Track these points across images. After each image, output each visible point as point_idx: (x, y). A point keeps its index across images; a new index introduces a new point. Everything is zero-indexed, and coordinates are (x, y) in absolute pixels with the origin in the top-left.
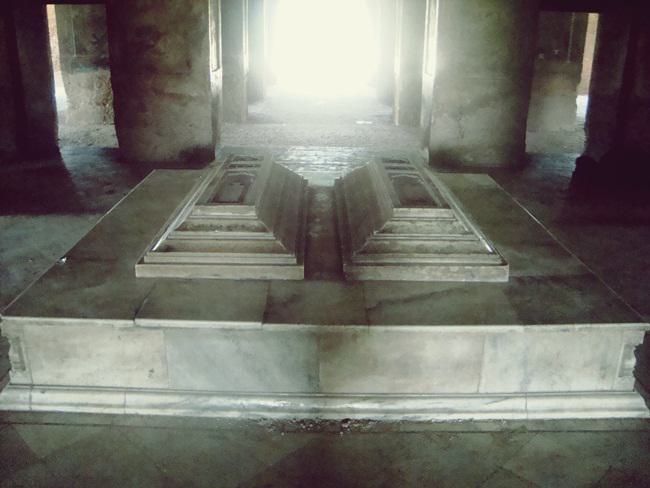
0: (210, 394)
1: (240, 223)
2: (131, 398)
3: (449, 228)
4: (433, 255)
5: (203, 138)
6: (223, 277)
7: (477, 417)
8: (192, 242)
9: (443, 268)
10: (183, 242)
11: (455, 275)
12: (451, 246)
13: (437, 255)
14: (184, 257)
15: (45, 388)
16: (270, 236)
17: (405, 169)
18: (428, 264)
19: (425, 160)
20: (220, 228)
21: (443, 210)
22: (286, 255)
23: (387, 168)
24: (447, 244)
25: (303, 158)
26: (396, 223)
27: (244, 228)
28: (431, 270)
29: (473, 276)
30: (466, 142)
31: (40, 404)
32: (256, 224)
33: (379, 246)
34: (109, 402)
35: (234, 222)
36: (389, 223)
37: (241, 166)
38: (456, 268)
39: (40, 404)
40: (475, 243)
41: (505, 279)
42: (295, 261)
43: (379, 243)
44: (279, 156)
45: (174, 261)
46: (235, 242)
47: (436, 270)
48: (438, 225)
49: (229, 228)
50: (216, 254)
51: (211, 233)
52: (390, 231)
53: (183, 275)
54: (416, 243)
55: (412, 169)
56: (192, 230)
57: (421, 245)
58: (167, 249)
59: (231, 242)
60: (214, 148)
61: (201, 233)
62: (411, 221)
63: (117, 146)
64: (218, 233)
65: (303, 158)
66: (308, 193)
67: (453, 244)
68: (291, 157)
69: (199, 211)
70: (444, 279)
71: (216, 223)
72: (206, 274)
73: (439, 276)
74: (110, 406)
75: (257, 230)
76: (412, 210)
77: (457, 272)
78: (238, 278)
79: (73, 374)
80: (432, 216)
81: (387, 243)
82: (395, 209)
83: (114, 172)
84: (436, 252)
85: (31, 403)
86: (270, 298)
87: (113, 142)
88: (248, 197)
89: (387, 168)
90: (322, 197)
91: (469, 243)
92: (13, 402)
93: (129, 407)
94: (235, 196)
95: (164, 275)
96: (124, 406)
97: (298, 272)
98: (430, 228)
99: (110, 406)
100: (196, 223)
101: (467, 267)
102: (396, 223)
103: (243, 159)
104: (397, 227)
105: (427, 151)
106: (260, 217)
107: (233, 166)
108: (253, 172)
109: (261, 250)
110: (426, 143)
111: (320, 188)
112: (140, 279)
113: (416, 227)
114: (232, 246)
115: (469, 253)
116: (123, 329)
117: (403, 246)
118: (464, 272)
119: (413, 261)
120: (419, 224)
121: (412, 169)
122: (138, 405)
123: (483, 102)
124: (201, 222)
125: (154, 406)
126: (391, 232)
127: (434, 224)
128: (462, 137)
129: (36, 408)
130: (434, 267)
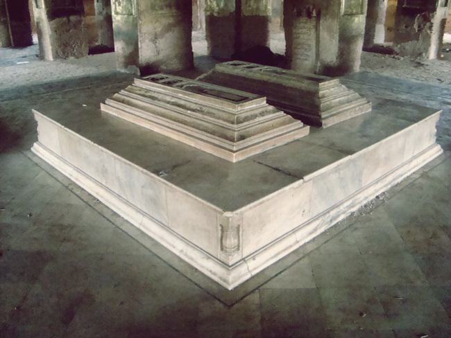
0: (328, 211)
2: (299, 235)
6: (277, 146)
7: (408, 174)
8: (251, 128)
10: (247, 130)
14: (254, 140)
15: (253, 256)
18: (349, 109)
20: (256, 116)
26: (324, 92)
27: (262, 114)
30: (160, 57)
31: (255, 269)
34: (289, 244)
39: (255, 269)
41: (370, 110)
53: (258, 152)
54: (337, 100)
61: (251, 122)
63: (135, 79)
71: (252, 113)
72: (269, 147)
74: (291, 246)
79: (265, 238)
80: (333, 84)
81: (328, 103)
85: (250, 272)
92: (240, 277)
93: (300, 240)
96: (297, 242)
99: (291, 246)
102: (324, 92)
112: (236, 163)
116: (300, 186)
119: (341, 110)
122: (303, 237)
123: (168, 28)
125: (311, 233)
129: (254, 273)
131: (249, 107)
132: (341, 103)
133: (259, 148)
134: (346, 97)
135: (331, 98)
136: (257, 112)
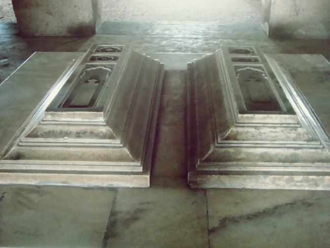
1: (89, 129)
3: (293, 135)
4: (276, 164)
5: (85, 16)
6: (71, 185)
8: (42, 149)
9: (286, 177)
10: (33, 149)
11: (299, 184)
12: (295, 155)
13: (281, 164)
16: (118, 142)
17: (249, 60)
19: (266, 33)
20: (67, 134)
21: (287, 116)
22: (132, 164)
23: (234, 60)
24: (292, 151)
25: (167, 32)
26: (240, 130)
27: (93, 134)
28: (275, 179)
29: (317, 185)
30: (300, 18)
32: (104, 130)
33: (225, 152)
35: (83, 128)
36: (233, 129)
37: (100, 59)
38: (300, 178)
40: (319, 151)
42: (141, 169)
43: (224, 150)
44: (147, 30)
45: (24, 168)
46: (83, 150)
47: (280, 179)
48: (282, 131)
49: (78, 135)
50: (65, 162)
51: (61, 140)
52: (234, 137)
53: (33, 182)
54: (259, 151)
55: (256, 61)
56: (42, 136)
57: (266, 153)
58: (18, 157)
59: (79, 149)
60: (95, 26)
61: (51, 140)
62: (255, 127)
64: (68, 140)
65: (167, 32)
66: (165, 76)
67: (299, 152)
68: (157, 31)
69: (49, 117)
70: (287, 187)
71: (66, 128)
72: (55, 181)
73: (282, 184)
75: (105, 136)
76: (257, 116)
77: (301, 181)
78: (86, 185)
81: (231, 150)
82: (240, 115)
83: (11, 46)
84: (280, 161)
86: (113, 214)
87: (16, 22)
88: (98, 104)
89: (234, 60)
90: (175, 82)
91: (313, 151)
94: (86, 98)
95: (15, 182)
97: (144, 181)
98: (273, 134)
100: (48, 128)
101: (311, 177)
103: (104, 50)
104: (241, 133)
105: (267, 24)
106: (108, 123)
107: (93, 59)
108: (111, 67)
109: (107, 158)
110: (266, 18)
111: (175, 72)
113: (260, 134)
114: (80, 154)
115: (313, 162)
117: (246, 152)
118: (307, 181)
120: (263, 130)
121: (256, 61)
124: (51, 128)
126: (235, 139)
127: (278, 130)
128: (297, 14)
130: (278, 176)
131: (69, 119)
132: (265, 158)
133: (35, 178)
134: (292, 151)
135: (245, 143)
136: (73, 129)
